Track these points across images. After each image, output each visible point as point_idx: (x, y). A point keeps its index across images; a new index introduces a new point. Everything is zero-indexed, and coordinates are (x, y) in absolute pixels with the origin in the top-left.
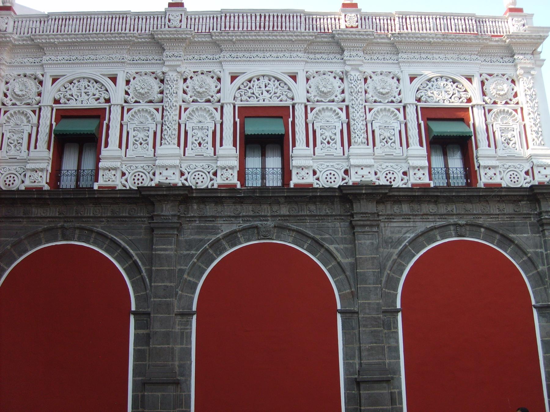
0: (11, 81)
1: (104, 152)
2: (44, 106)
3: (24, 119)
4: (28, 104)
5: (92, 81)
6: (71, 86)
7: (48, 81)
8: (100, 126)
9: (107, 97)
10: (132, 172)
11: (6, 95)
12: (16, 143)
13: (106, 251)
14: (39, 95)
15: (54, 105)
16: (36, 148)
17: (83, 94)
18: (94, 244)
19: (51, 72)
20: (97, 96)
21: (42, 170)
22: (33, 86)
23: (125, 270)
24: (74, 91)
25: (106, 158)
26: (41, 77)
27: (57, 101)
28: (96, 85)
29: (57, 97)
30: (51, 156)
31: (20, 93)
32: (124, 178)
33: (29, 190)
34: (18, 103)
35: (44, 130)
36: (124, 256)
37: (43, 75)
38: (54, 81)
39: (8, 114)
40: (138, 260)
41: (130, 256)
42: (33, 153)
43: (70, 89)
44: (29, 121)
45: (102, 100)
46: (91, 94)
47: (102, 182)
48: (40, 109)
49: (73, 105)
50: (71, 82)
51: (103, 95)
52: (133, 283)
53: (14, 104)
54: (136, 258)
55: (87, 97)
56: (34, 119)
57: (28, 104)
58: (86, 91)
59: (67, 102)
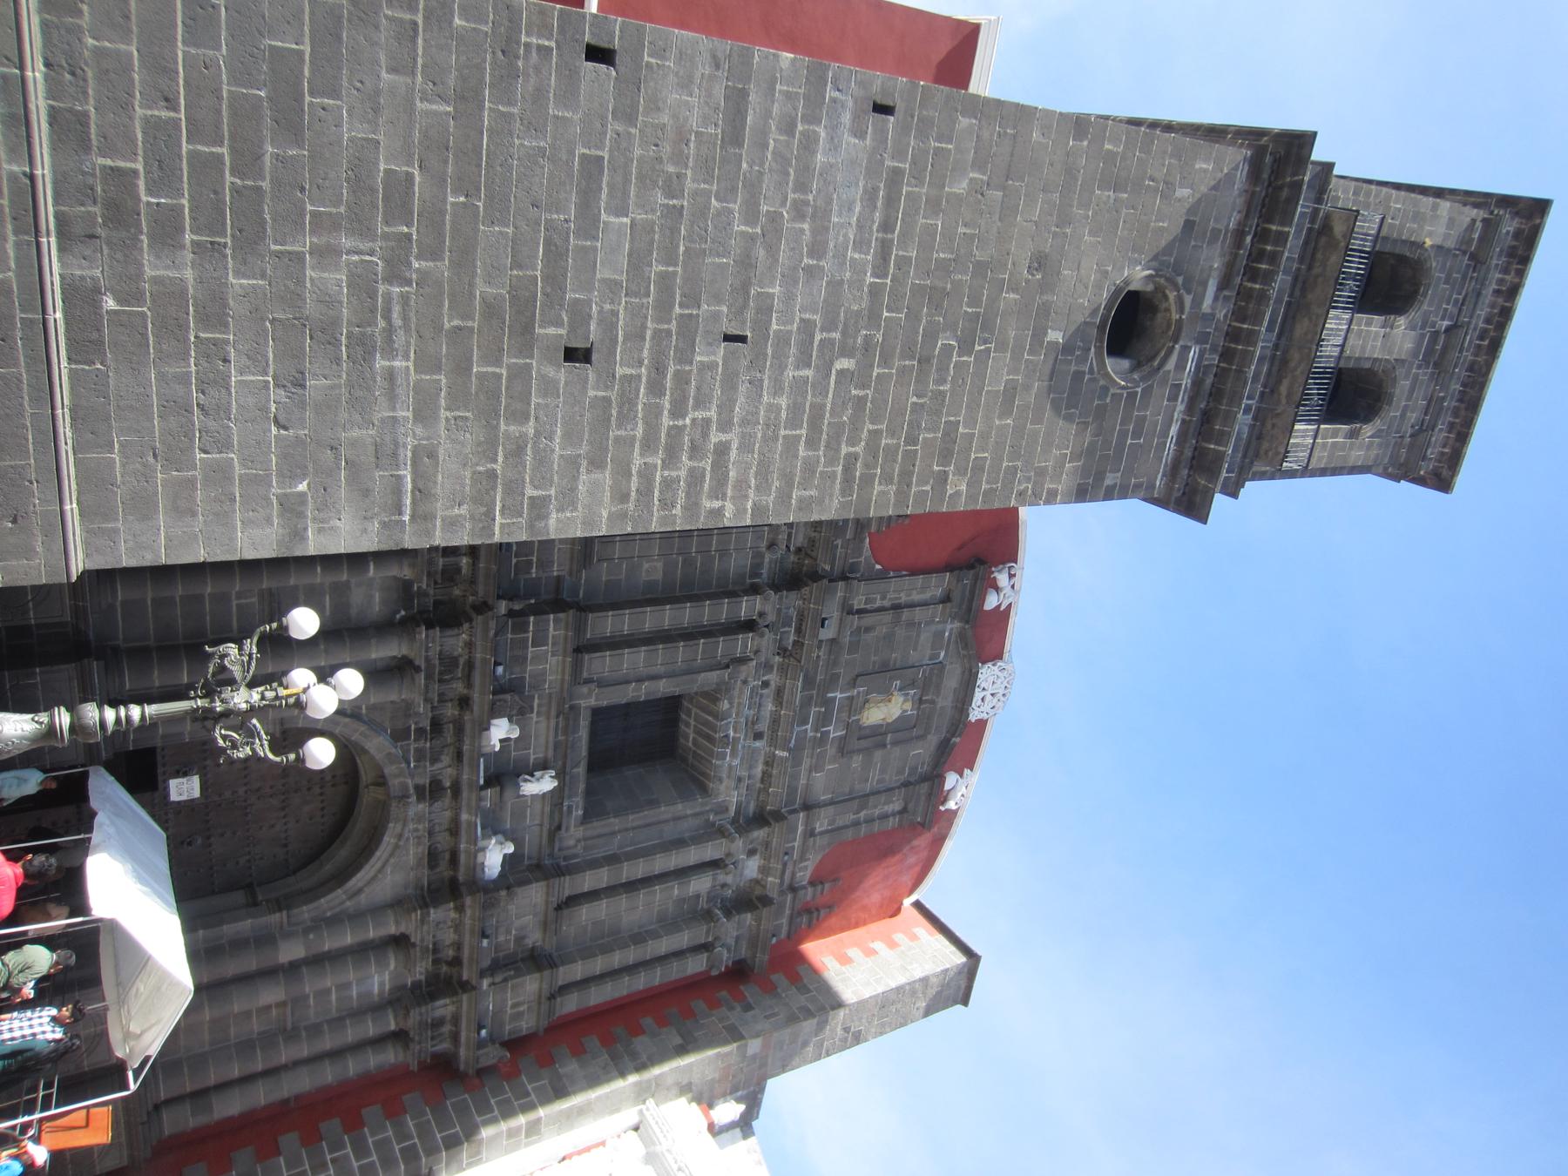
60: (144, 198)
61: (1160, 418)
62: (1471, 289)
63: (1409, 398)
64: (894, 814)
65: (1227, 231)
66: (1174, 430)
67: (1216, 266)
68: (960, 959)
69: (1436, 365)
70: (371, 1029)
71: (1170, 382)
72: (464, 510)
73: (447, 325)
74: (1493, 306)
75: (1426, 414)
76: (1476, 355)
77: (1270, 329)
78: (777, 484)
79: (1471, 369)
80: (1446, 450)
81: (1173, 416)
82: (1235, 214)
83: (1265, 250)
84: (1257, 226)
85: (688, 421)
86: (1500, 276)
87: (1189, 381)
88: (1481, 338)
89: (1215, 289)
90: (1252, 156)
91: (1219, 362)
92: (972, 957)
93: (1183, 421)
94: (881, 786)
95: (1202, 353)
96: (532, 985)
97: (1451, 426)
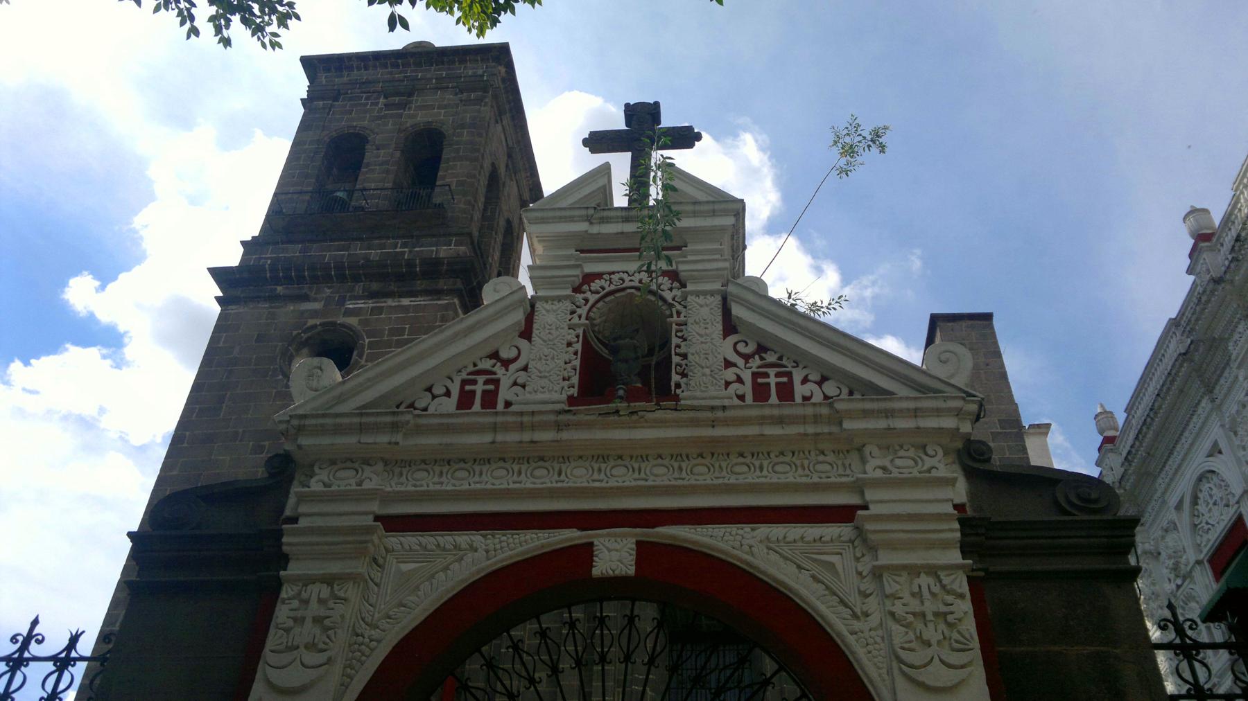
62: (359, 91)
63: (432, 107)
66: (406, 302)
69: (410, 94)
71: (368, 317)
75: (448, 88)
76: (409, 65)
79: (418, 64)
81: (395, 307)
82: (260, 305)
87: (370, 302)
89: (308, 303)
91: (362, 282)
93: (400, 296)
95: (352, 298)
97: (462, 61)
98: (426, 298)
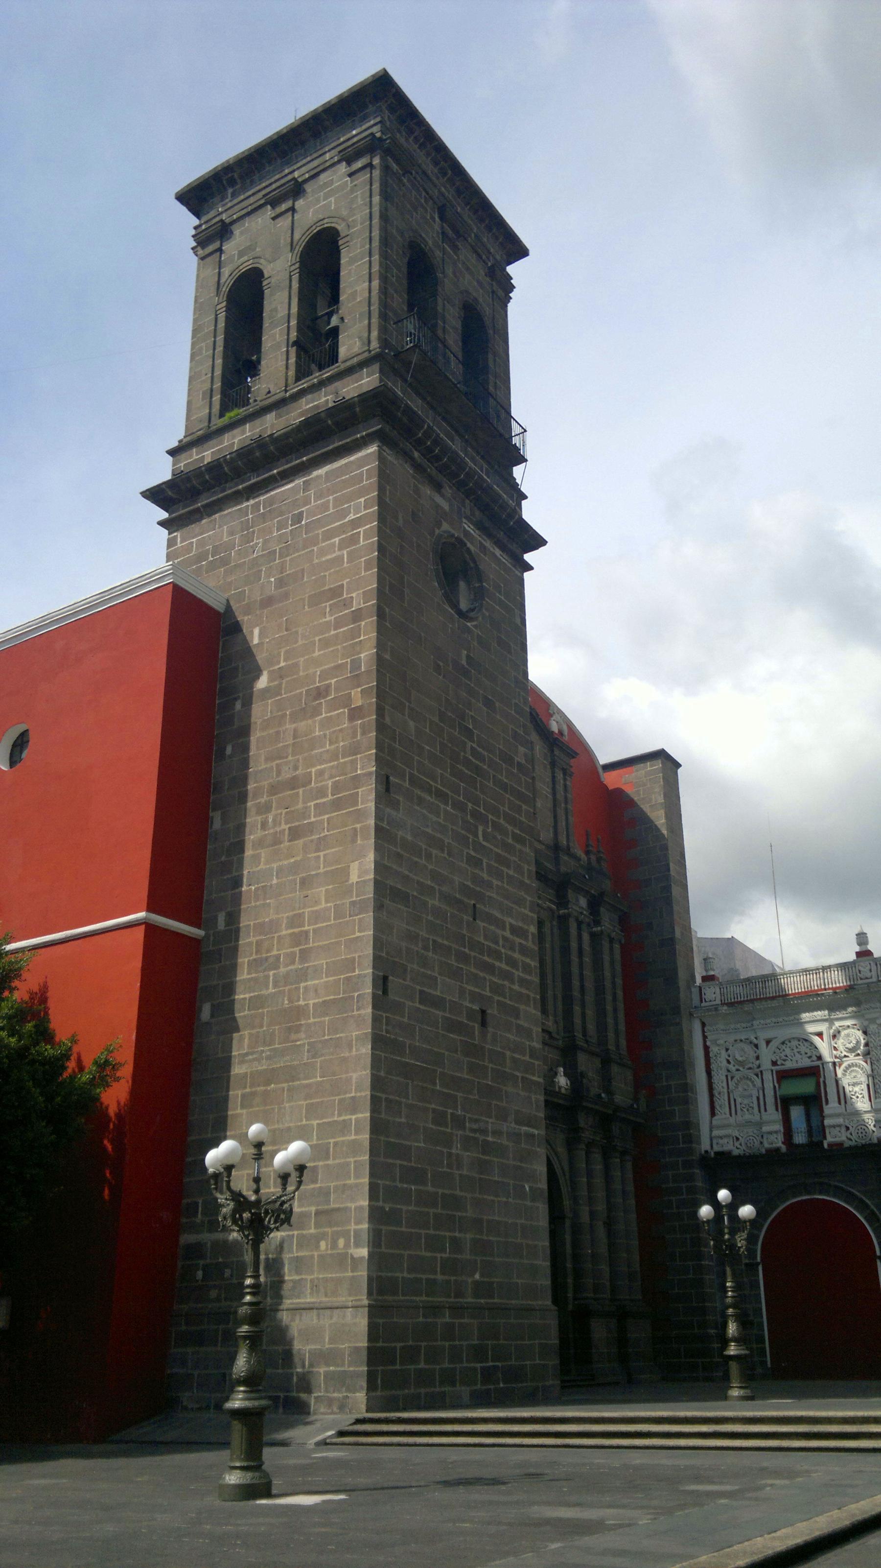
0: (731, 1047)
1: (827, 1110)
2: (765, 1070)
3: (750, 1083)
4: (750, 1068)
5: (801, 1040)
6: (784, 1047)
7: (763, 1045)
8: (818, 1084)
9: (818, 1055)
10: (855, 1126)
11: (729, 1062)
12: (747, 1107)
13: (846, 1202)
14: (758, 1058)
15: (773, 1068)
16: (766, 1110)
17: (797, 1054)
18: (834, 1196)
19: (763, 1035)
20: (809, 1055)
21: (776, 1132)
22: (750, 1051)
23: (865, 1218)
24: (788, 1051)
25: (831, 1116)
26: (755, 1041)
27: (774, 1063)
28: (806, 1044)
29: (774, 1060)
30: (781, 1117)
31: (740, 1059)
32: (849, 1132)
33: (769, 1151)
34: (741, 1069)
35: (770, 1093)
36: (862, 1206)
37: (756, 1038)
38: (768, 1042)
39: (735, 1079)
40: (875, 1210)
41: (867, 1206)
42: (765, 1117)
43: (784, 1050)
44: (754, 1085)
45: (815, 1058)
46: (803, 1053)
47: (830, 1139)
48: (761, 1072)
49: (789, 1065)
50: (783, 1043)
51: (814, 1053)
52: (874, 1230)
53: (738, 1070)
54: (872, 1207)
55: (800, 1056)
56: (758, 1082)
57: (750, 1068)
58: (798, 1050)
59: (783, 1062)
60: (447, 1255)
61: (493, 565)
64: (565, 780)
65: (413, 477)
67: (429, 492)
68: (658, 765)
70: (598, 1167)
72: (533, 1097)
73: (477, 1097)
74: (428, 154)
77: (452, 440)
78: (523, 893)
80: (501, 240)
83: (419, 438)
84: (410, 443)
85: (503, 951)
86: (412, 138)
88: (445, 174)
90: (381, 442)
92: (661, 755)
94: (551, 785)
96: (615, 1069)
98: (510, 561)
